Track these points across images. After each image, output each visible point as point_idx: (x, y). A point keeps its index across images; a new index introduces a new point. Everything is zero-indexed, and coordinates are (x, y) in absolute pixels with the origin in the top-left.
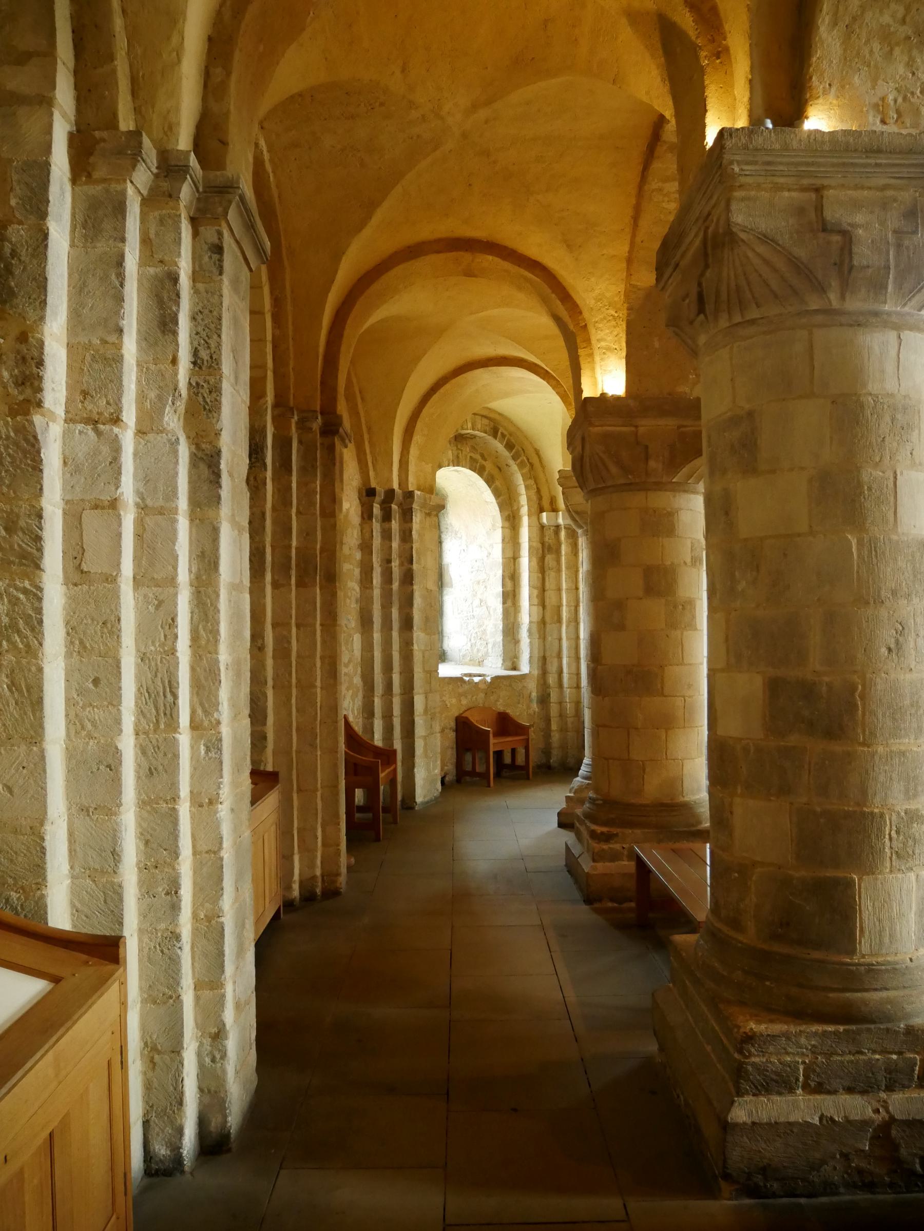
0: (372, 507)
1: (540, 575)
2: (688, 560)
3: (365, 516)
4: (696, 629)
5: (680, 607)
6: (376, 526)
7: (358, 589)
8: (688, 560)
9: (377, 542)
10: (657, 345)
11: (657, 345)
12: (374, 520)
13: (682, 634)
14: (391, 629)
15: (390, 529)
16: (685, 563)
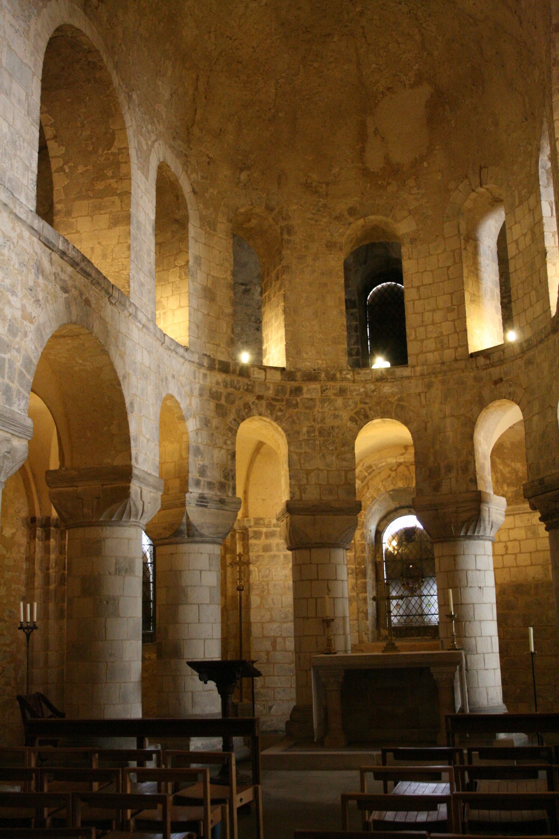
0: (35, 531)
1: (222, 571)
2: (113, 570)
3: (32, 537)
4: (117, 615)
5: (105, 603)
6: (38, 544)
7: (23, 589)
8: (113, 570)
9: (38, 555)
10: (89, 435)
11: (89, 435)
12: (37, 540)
13: (106, 620)
14: (48, 619)
15: (49, 545)
16: (110, 573)
